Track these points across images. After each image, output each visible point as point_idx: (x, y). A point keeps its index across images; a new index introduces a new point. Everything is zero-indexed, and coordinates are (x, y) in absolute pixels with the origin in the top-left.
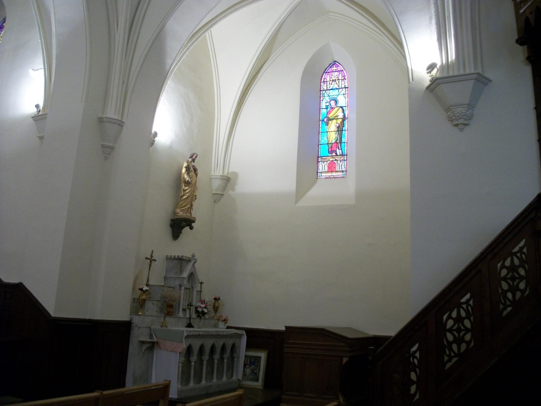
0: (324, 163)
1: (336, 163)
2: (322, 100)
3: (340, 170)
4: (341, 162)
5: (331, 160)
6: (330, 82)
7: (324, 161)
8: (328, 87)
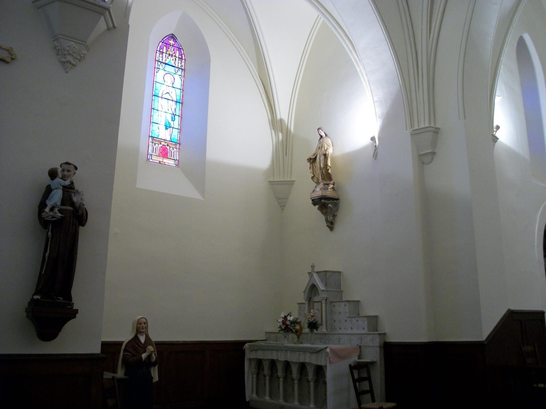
2: (157, 72)
3: (172, 158)
4: (173, 149)
6: (166, 54)
7: (155, 143)
8: (164, 59)
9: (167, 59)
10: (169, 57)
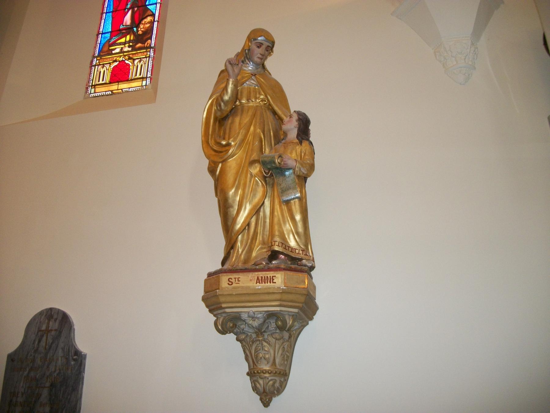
0: (103, 67)
4: (140, 61)
5: (121, 59)
7: (103, 64)
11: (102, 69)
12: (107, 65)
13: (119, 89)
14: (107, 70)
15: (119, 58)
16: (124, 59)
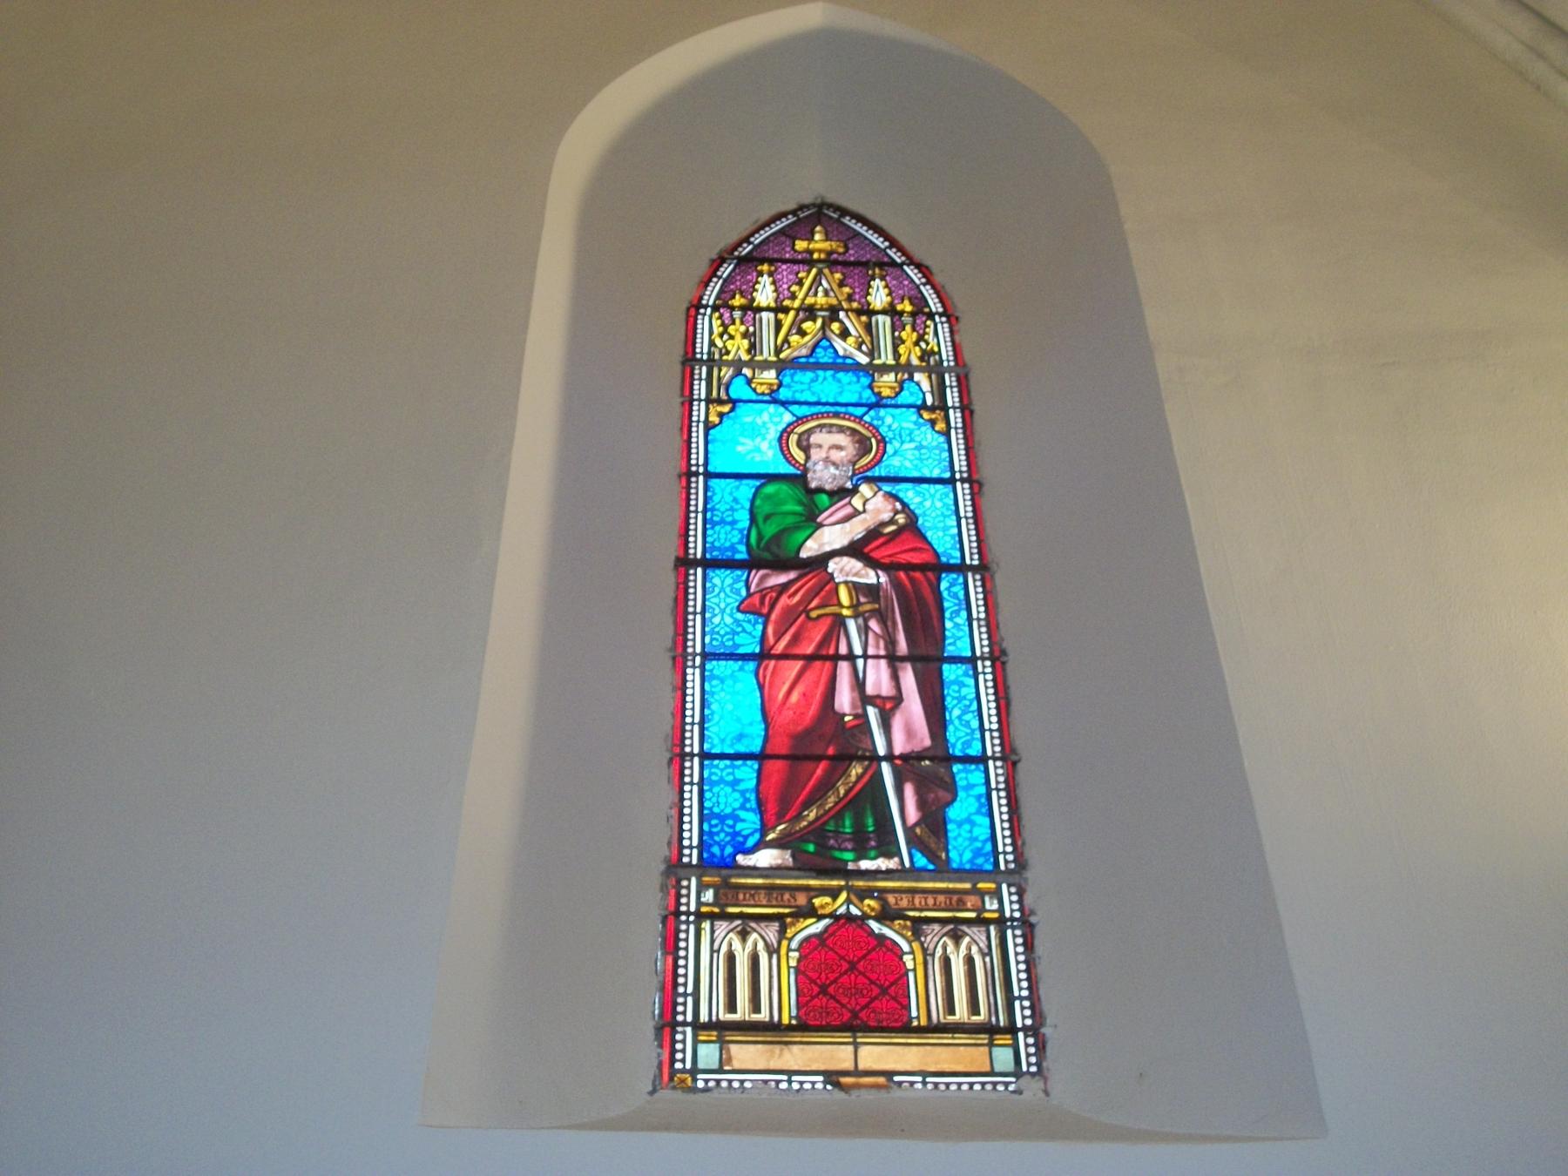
1: (905, 947)
5: (840, 905)
8: (768, 340)
9: (794, 339)
10: (807, 326)
11: (737, 945)
12: (763, 925)
13: (861, 1066)
14: (775, 956)
15: (828, 900)
16: (854, 911)
